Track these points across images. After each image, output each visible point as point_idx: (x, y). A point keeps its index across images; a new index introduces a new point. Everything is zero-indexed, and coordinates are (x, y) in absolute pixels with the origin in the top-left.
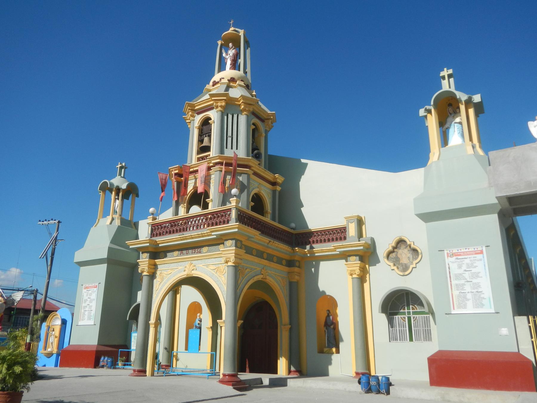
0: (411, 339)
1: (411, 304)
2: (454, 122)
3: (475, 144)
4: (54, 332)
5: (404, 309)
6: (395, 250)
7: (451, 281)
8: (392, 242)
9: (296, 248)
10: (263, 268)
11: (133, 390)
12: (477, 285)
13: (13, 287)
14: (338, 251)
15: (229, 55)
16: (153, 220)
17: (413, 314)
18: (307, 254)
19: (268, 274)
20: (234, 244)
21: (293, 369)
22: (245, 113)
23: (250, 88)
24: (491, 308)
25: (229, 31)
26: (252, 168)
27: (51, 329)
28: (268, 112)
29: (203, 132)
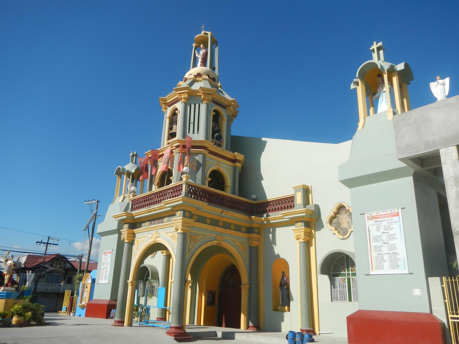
0: (350, 300)
1: (350, 266)
2: (383, 91)
3: (398, 111)
4: (87, 289)
5: (345, 271)
6: (337, 215)
7: (370, 243)
8: (334, 209)
9: (252, 217)
10: (219, 235)
11: (73, 337)
12: (393, 247)
13: (67, 254)
14: (286, 218)
15: (200, 54)
16: (133, 197)
17: (352, 276)
18: (264, 222)
19: (223, 240)
20: (182, 214)
21: (251, 324)
22: (205, 102)
23: (216, 80)
24: (405, 269)
25: (201, 34)
26: (209, 148)
27: (85, 287)
28: (229, 100)
29: (173, 121)
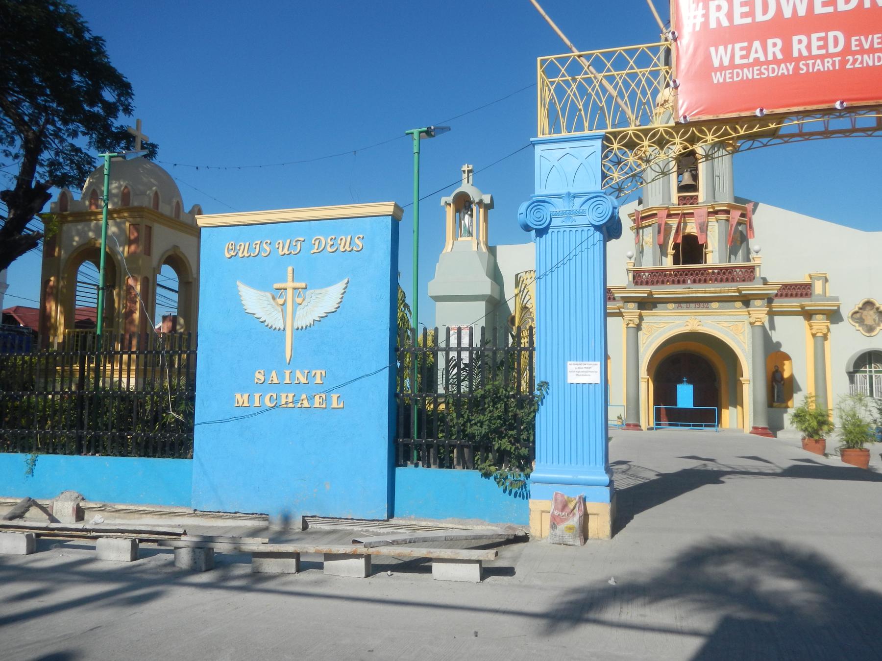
6: (860, 311)
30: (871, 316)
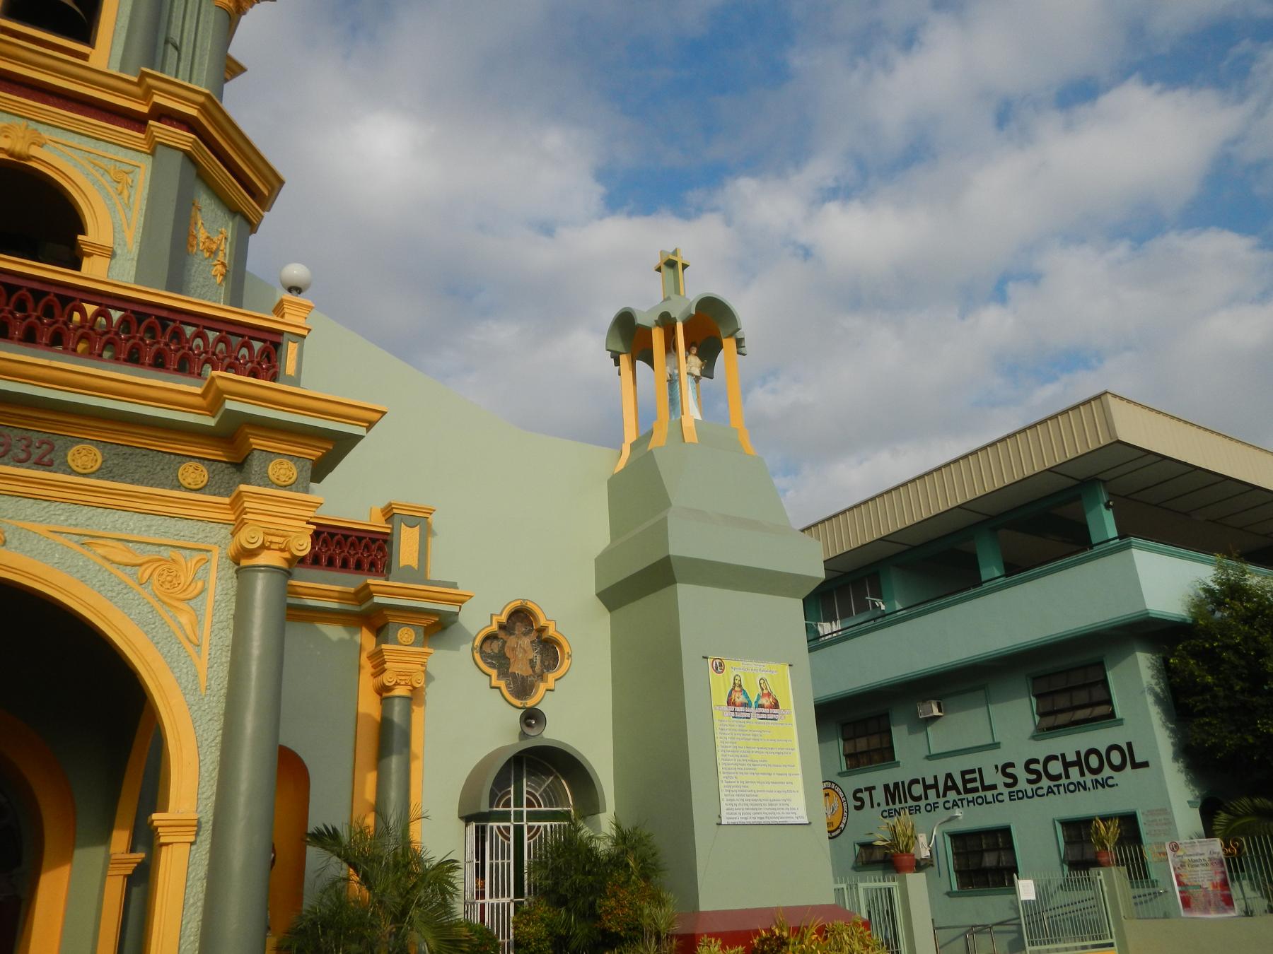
5: (507, 804)
6: (502, 635)
17: (529, 819)
30: (525, 651)
